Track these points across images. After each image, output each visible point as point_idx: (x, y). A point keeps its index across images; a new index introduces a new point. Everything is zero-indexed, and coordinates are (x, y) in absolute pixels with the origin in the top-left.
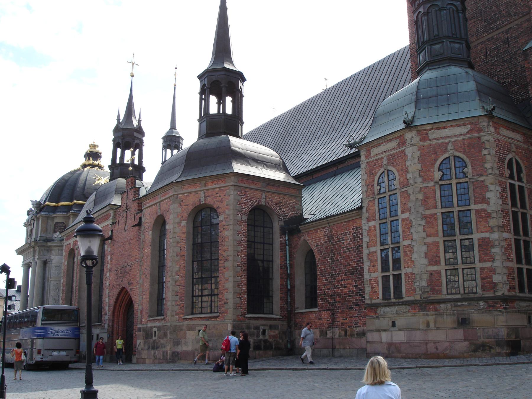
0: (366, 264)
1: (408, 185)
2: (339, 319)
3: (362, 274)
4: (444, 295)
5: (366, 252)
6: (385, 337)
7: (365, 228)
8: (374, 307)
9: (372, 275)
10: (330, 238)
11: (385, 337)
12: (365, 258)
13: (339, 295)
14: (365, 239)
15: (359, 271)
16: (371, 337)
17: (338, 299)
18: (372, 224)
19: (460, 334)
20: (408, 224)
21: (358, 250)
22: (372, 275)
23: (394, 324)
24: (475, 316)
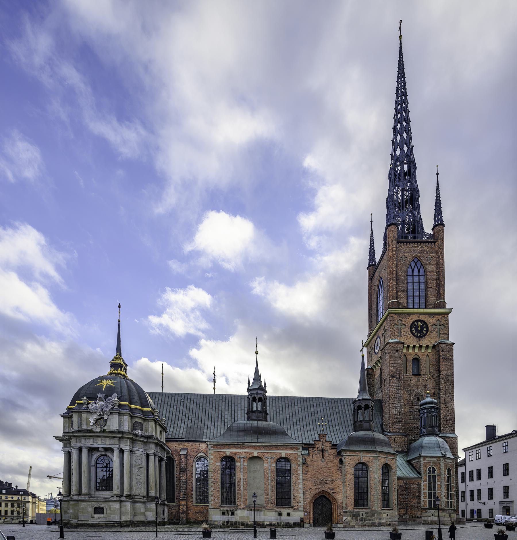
0: (422, 496)
1: (441, 474)
2: (409, 512)
3: (420, 498)
4: (447, 508)
5: (422, 492)
6: (429, 519)
7: (422, 484)
8: (425, 509)
9: (425, 500)
10: (406, 484)
11: (429, 519)
12: (422, 493)
13: (409, 504)
14: (422, 487)
15: (419, 497)
16: (423, 518)
17: (408, 505)
18: (425, 483)
19: (449, 519)
20: (440, 486)
21: (419, 490)
22: (425, 500)
23: (433, 515)
24: (452, 514)
